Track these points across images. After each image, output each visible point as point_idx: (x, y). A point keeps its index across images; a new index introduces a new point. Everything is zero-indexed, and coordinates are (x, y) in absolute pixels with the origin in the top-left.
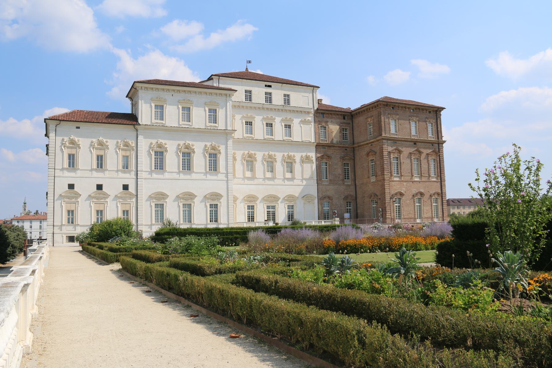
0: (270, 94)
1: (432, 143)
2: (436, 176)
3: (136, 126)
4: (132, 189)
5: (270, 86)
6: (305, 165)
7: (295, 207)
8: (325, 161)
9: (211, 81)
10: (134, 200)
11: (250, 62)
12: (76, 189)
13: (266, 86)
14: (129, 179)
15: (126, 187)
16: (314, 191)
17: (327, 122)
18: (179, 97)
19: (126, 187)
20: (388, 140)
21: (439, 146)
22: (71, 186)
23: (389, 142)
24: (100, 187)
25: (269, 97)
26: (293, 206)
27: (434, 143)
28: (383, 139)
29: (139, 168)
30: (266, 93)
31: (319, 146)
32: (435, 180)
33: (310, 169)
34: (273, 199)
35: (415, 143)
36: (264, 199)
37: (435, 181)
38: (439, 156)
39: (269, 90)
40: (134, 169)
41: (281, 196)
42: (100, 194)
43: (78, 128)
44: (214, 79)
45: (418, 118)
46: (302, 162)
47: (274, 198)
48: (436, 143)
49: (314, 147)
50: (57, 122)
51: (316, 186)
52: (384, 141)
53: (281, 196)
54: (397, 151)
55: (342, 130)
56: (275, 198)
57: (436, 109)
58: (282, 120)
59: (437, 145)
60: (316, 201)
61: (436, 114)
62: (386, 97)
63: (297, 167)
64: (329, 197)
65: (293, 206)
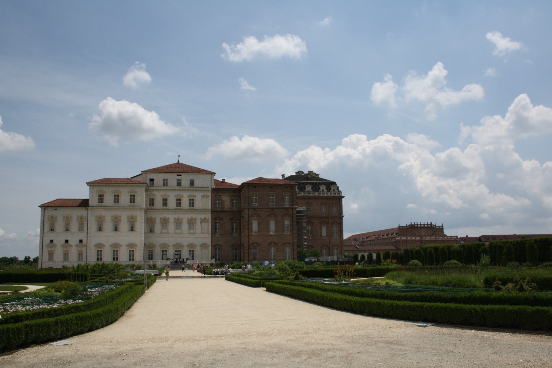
0: (181, 180)
1: (287, 209)
2: (289, 231)
3: (87, 208)
4: (84, 242)
5: (180, 175)
6: (204, 224)
7: (194, 251)
8: (217, 221)
9: (141, 176)
10: (85, 248)
11: (179, 156)
12: (54, 242)
13: (178, 175)
14: (83, 236)
15: (81, 241)
16: (209, 241)
17: (221, 195)
18: (113, 189)
19: (81, 241)
20: (248, 208)
21: (292, 211)
22: (52, 241)
23: (250, 209)
24: (67, 241)
25: (179, 183)
26: (193, 250)
27: (288, 209)
28: (245, 208)
29: (88, 230)
30: (178, 180)
31: (213, 211)
32: (289, 234)
33: (208, 227)
34: (179, 246)
35: (272, 209)
36: (174, 246)
37: (288, 235)
38: (292, 217)
39: (179, 178)
40: (86, 231)
41: (185, 244)
42: (67, 245)
43: (56, 210)
44: (143, 174)
45: (275, 193)
46: (201, 222)
47: (180, 245)
48: (290, 209)
49: (210, 213)
50: (44, 208)
51: (211, 238)
52: (246, 209)
53: (185, 244)
54: (256, 215)
55: (232, 201)
56: (182, 246)
57: (291, 185)
58: (188, 196)
59: (291, 210)
60: (210, 248)
61: (292, 188)
62: (261, 179)
63: (198, 226)
64: (219, 245)
65: (193, 250)
